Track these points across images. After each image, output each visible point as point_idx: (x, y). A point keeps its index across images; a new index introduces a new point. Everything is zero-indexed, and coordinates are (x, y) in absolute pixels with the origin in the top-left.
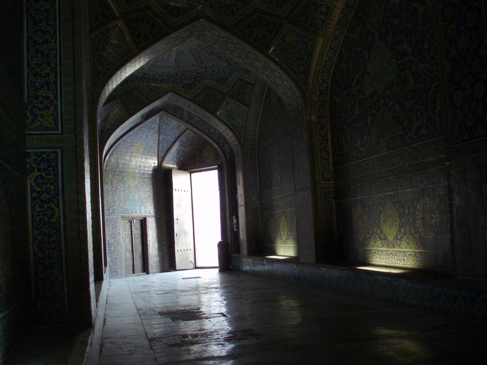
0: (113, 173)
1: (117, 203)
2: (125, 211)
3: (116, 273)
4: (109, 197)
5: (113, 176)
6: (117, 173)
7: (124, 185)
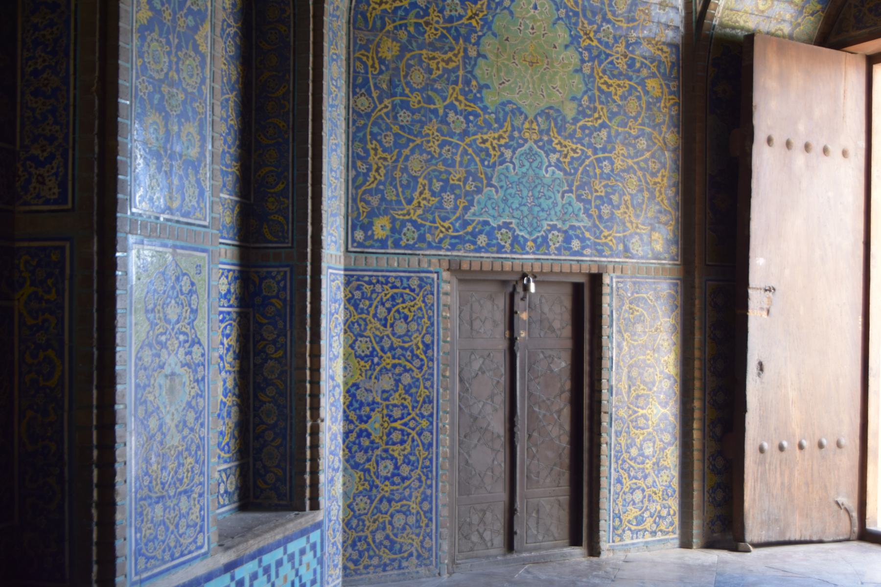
0: (403, 35)
1: (424, 198)
2: (474, 235)
3: (387, 556)
4: (373, 159)
5: (404, 49)
6: (430, 35)
7: (475, 100)
